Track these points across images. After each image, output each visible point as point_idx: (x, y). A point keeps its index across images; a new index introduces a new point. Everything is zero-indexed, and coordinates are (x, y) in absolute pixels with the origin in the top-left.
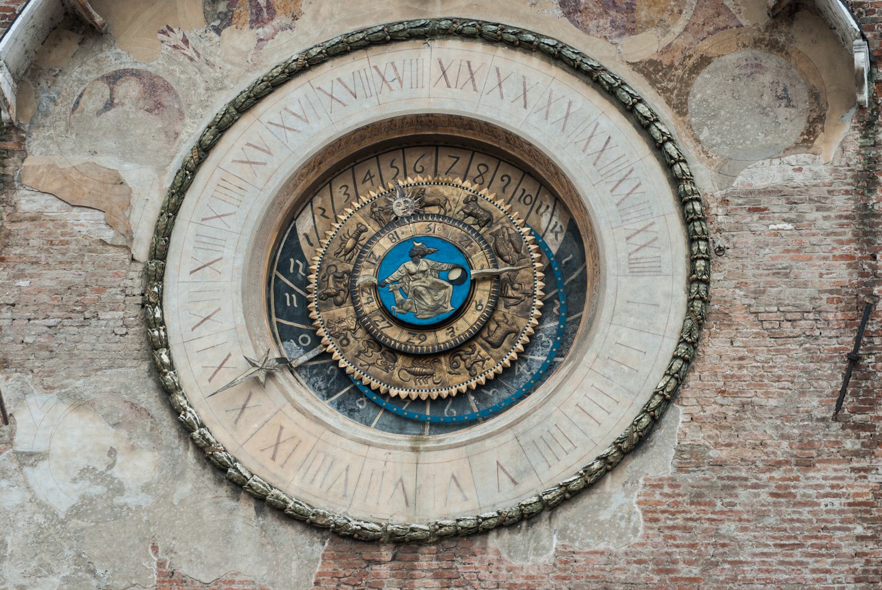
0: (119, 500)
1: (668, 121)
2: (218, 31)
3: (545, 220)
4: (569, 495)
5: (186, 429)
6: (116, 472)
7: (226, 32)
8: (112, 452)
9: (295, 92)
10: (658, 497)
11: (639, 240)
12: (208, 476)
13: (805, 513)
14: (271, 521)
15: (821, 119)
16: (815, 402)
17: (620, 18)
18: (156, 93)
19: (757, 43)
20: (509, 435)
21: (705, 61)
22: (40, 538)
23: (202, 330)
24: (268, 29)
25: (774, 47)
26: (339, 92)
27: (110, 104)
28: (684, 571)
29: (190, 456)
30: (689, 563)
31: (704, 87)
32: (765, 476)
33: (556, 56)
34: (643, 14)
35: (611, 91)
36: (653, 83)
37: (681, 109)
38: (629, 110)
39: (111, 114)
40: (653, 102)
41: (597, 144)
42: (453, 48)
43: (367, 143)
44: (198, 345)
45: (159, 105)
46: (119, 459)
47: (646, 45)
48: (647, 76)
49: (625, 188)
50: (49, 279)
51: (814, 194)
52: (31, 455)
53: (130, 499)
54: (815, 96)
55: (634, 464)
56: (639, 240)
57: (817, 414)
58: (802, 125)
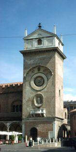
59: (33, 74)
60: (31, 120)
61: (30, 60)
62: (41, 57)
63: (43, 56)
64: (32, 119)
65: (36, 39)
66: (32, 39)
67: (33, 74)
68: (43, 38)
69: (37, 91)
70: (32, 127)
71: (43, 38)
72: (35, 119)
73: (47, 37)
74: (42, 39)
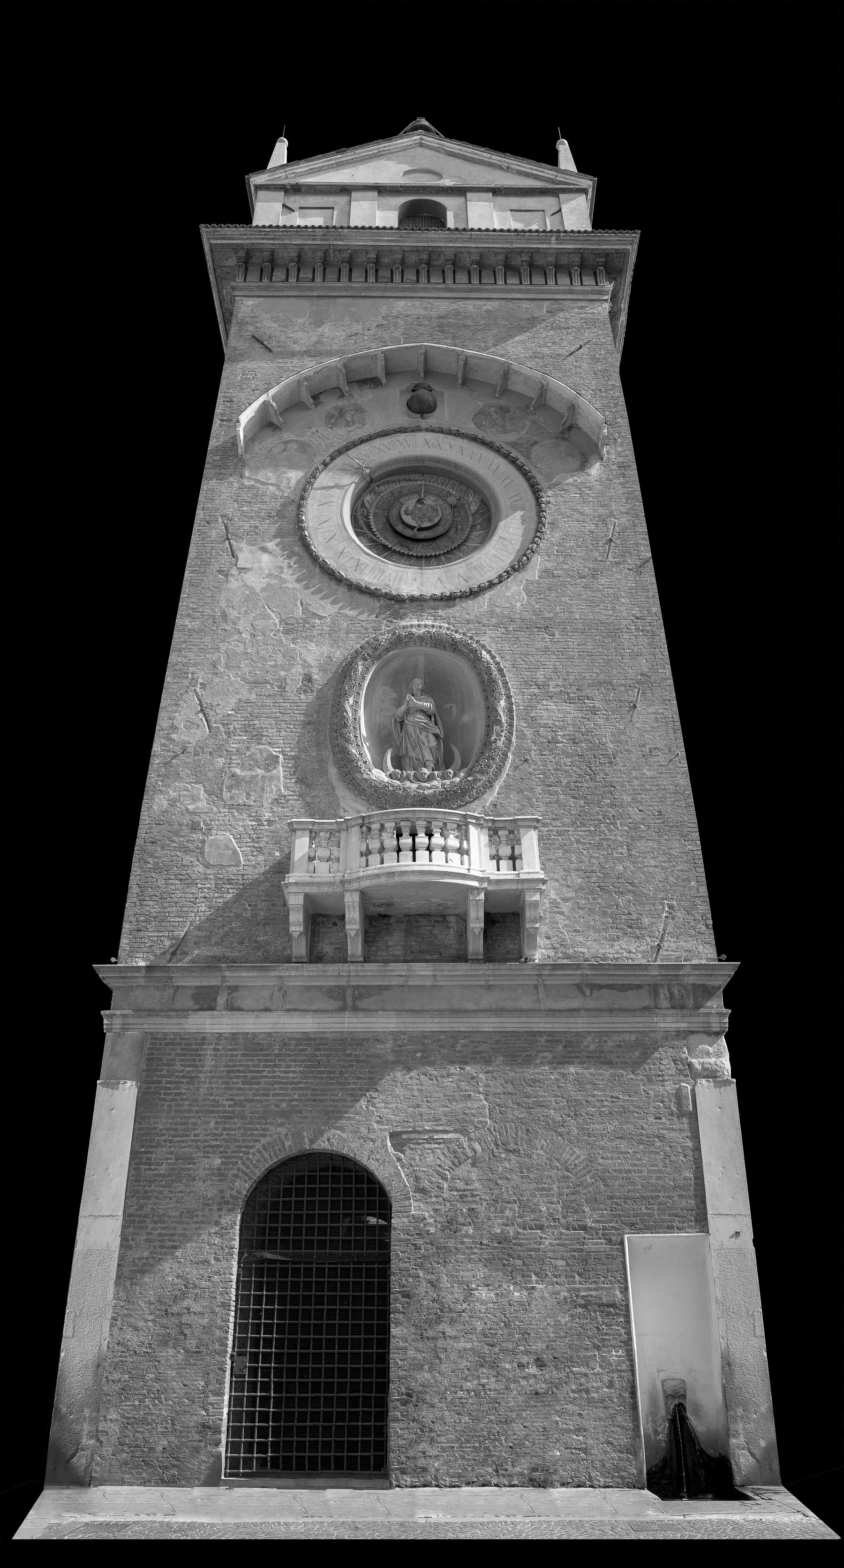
0: (284, 585)
1: (522, 460)
2: (331, 428)
3: (471, 498)
4: (491, 585)
5: (315, 558)
6: (283, 576)
7: (334, 429)
8: (281, 568)
9: (364, 448)
10: (532, 587)
11: (514, 499)
12: (325, 578)
13: (599, 594)
14: (356, 594)
15: (586, 461)
16: (598, 554)
17: (499, 429)
18: (303, 447)
19: (557, 438)
20: (463, 564)
21: (536, 443)
22: (247, 599)
23: (324, 525)
24: (352, 428)
25: (563, 439)
26: (382, 447)
27: (285, 450)
28: (547, 615)
29: (317, 570)
30: (548, 612)
31: (536, 451)
32: (579, 581)
33: (474, 439)
34: (509, 428)
35: (498, 450)
36: (516, 449)
37: (528, 457)
38: (506, 456)
39: (285, 454)
40: (514, 454)
41: (494, 467)
42: (430, 436)
43: (394, 467)
44: (321, 531)
45: (305, 451)
46: (285, 570)
47: (512, 437)
48: (513, 447)
49: (507, 482)
50: (256, 508)
51: (587, 485)
52: (244, 569)
53: (290, 586)
54: (583, 454)
55: (520, 576)
56: (514, 499)
57: (599, 558)
58: (579, 463)
59: (340, 435)
60: (277, 1012)
61: (319, 323)
62: (443, 307)
63: (470, 306)
64: (283, 1000)
65: (382, 190)
66: (345, 190)
67: (340, 435)
68: (460, 191)
69: (396, 603)
70: (279, 1141)
71: (460, 191)
72: (348, 999)
73: (496, 192)
74: (449, 203)
